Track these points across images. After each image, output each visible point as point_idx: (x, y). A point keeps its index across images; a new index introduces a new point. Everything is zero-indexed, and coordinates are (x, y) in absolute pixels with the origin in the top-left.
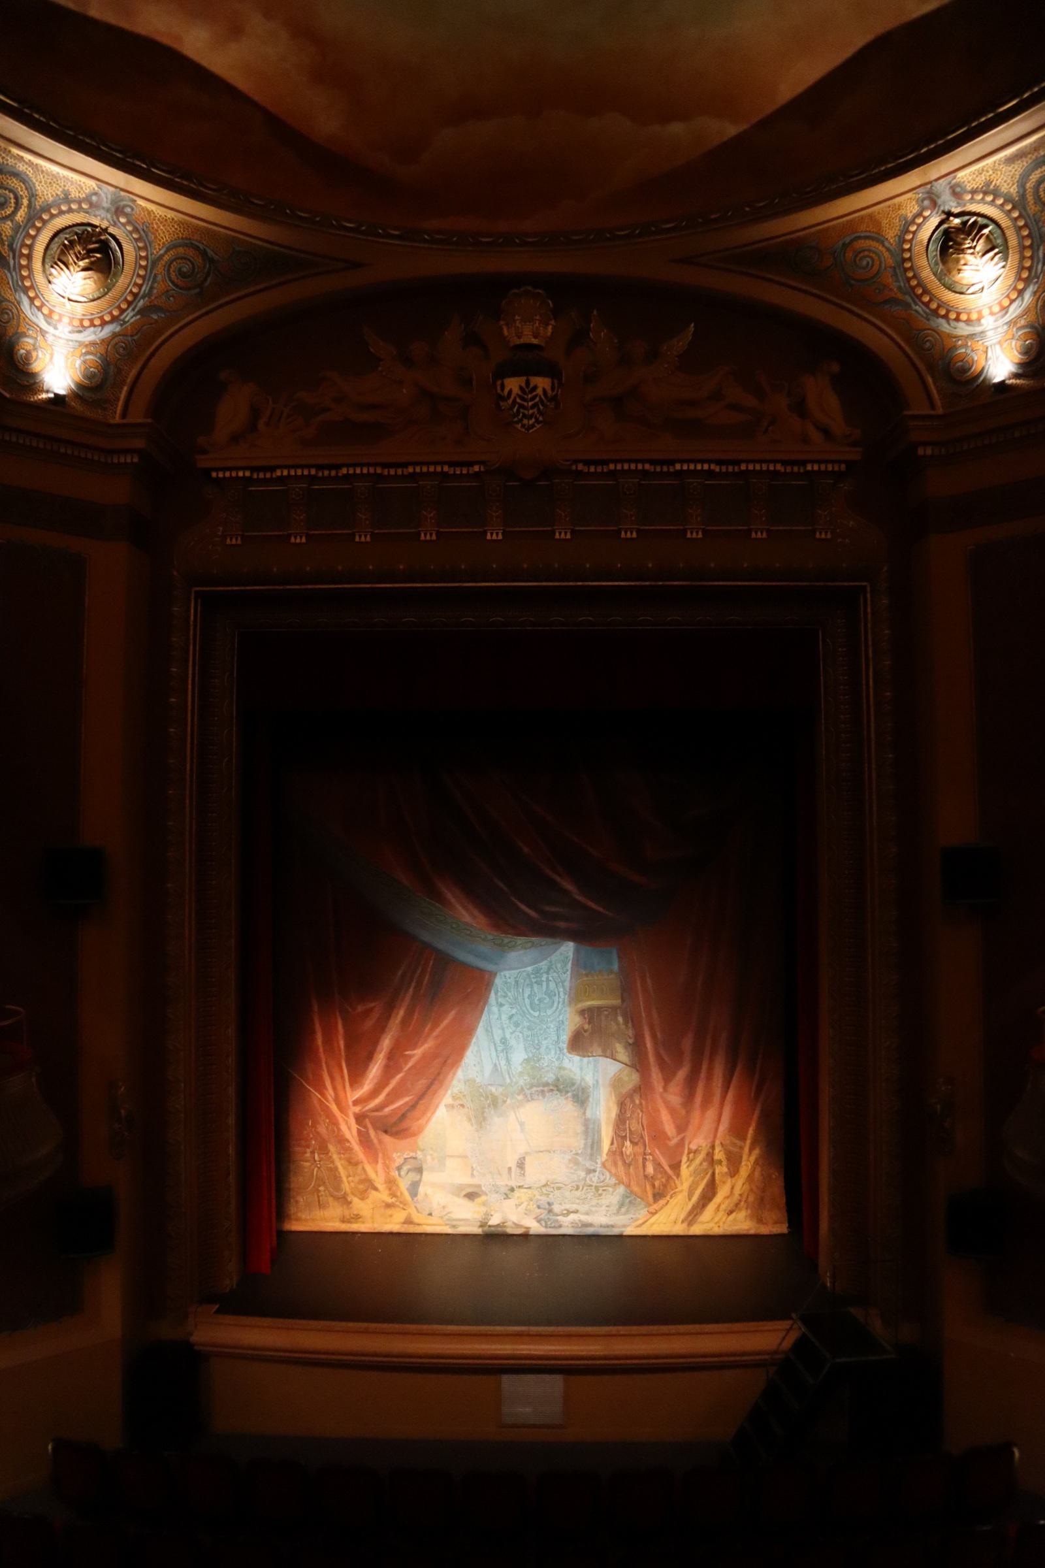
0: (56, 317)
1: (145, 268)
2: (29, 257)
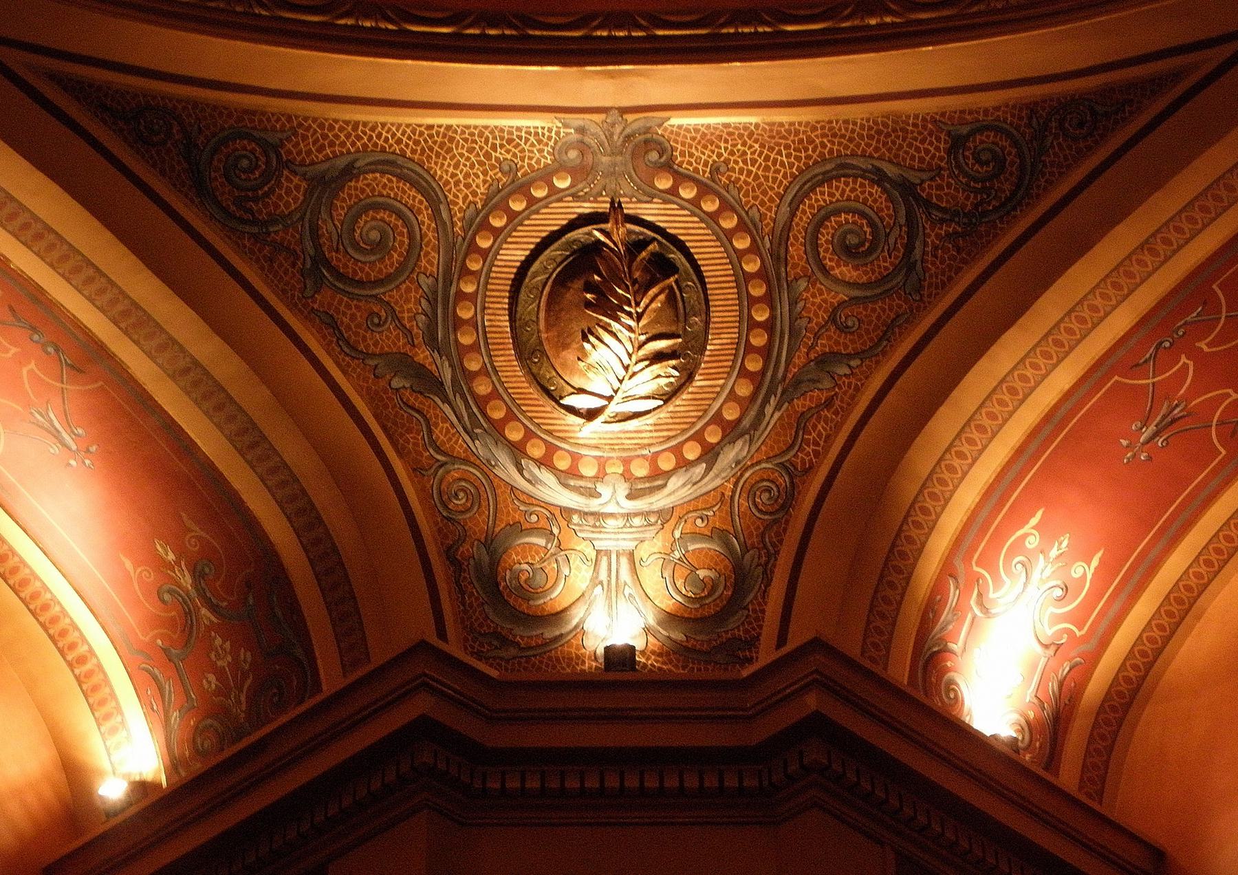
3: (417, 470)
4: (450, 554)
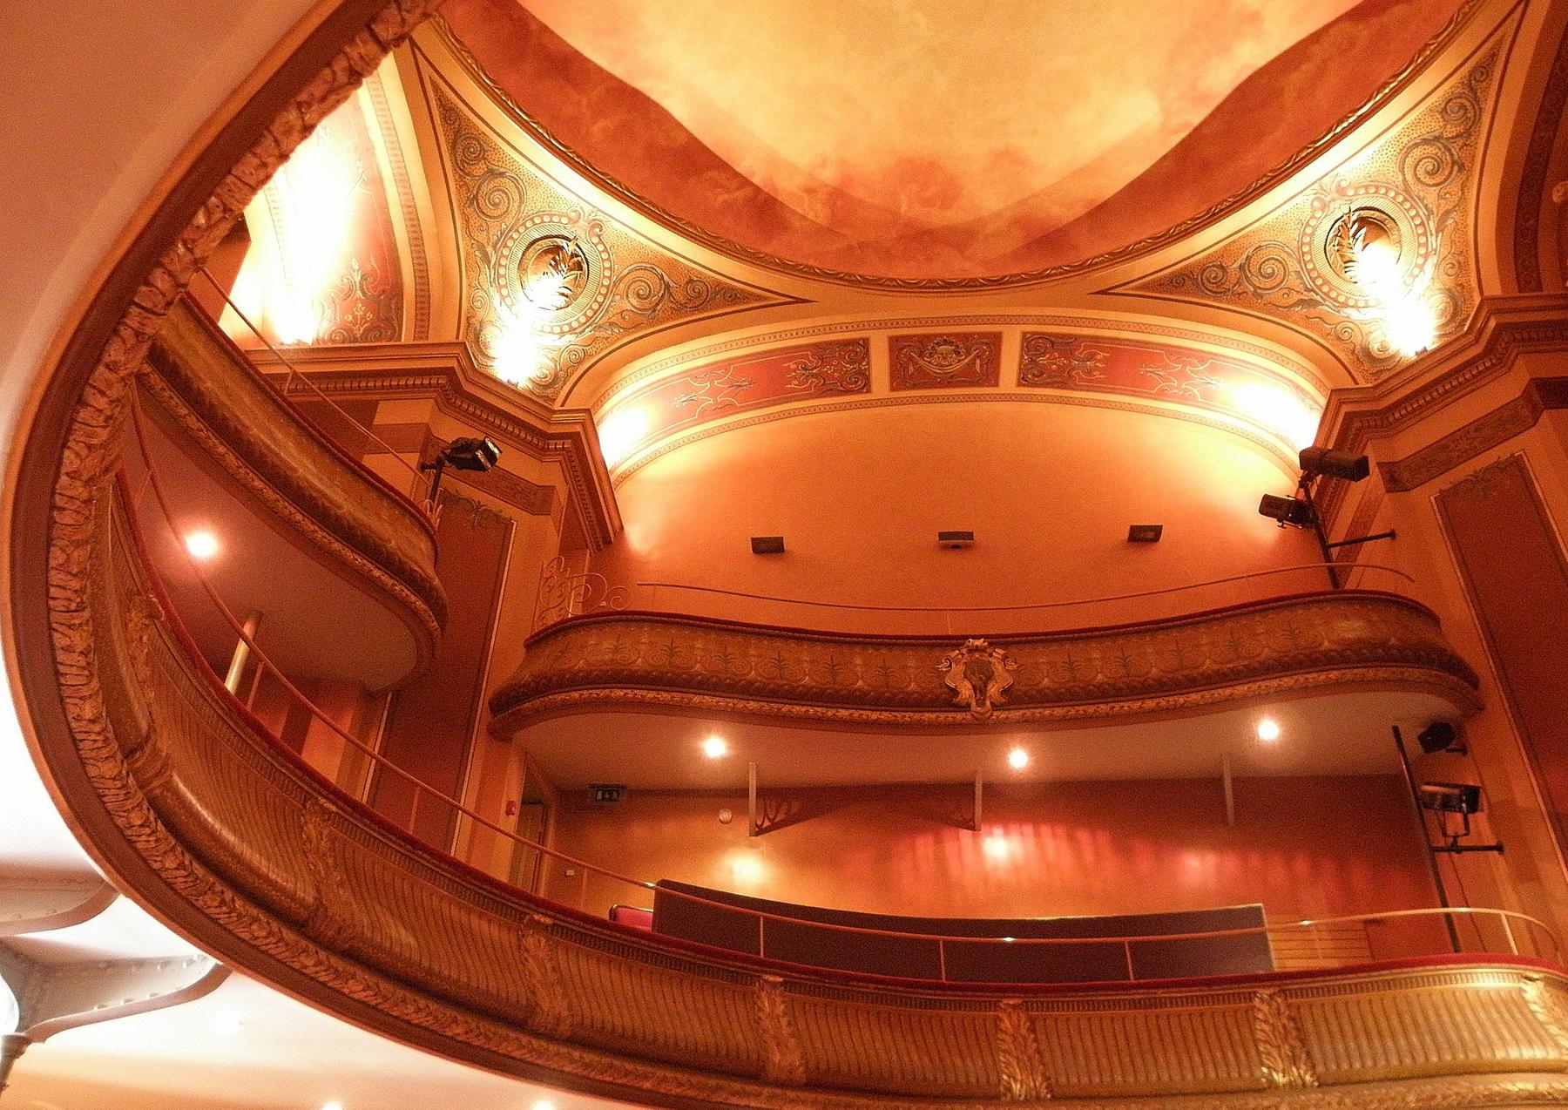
1: (1405, 200)
2: (1326, 282)
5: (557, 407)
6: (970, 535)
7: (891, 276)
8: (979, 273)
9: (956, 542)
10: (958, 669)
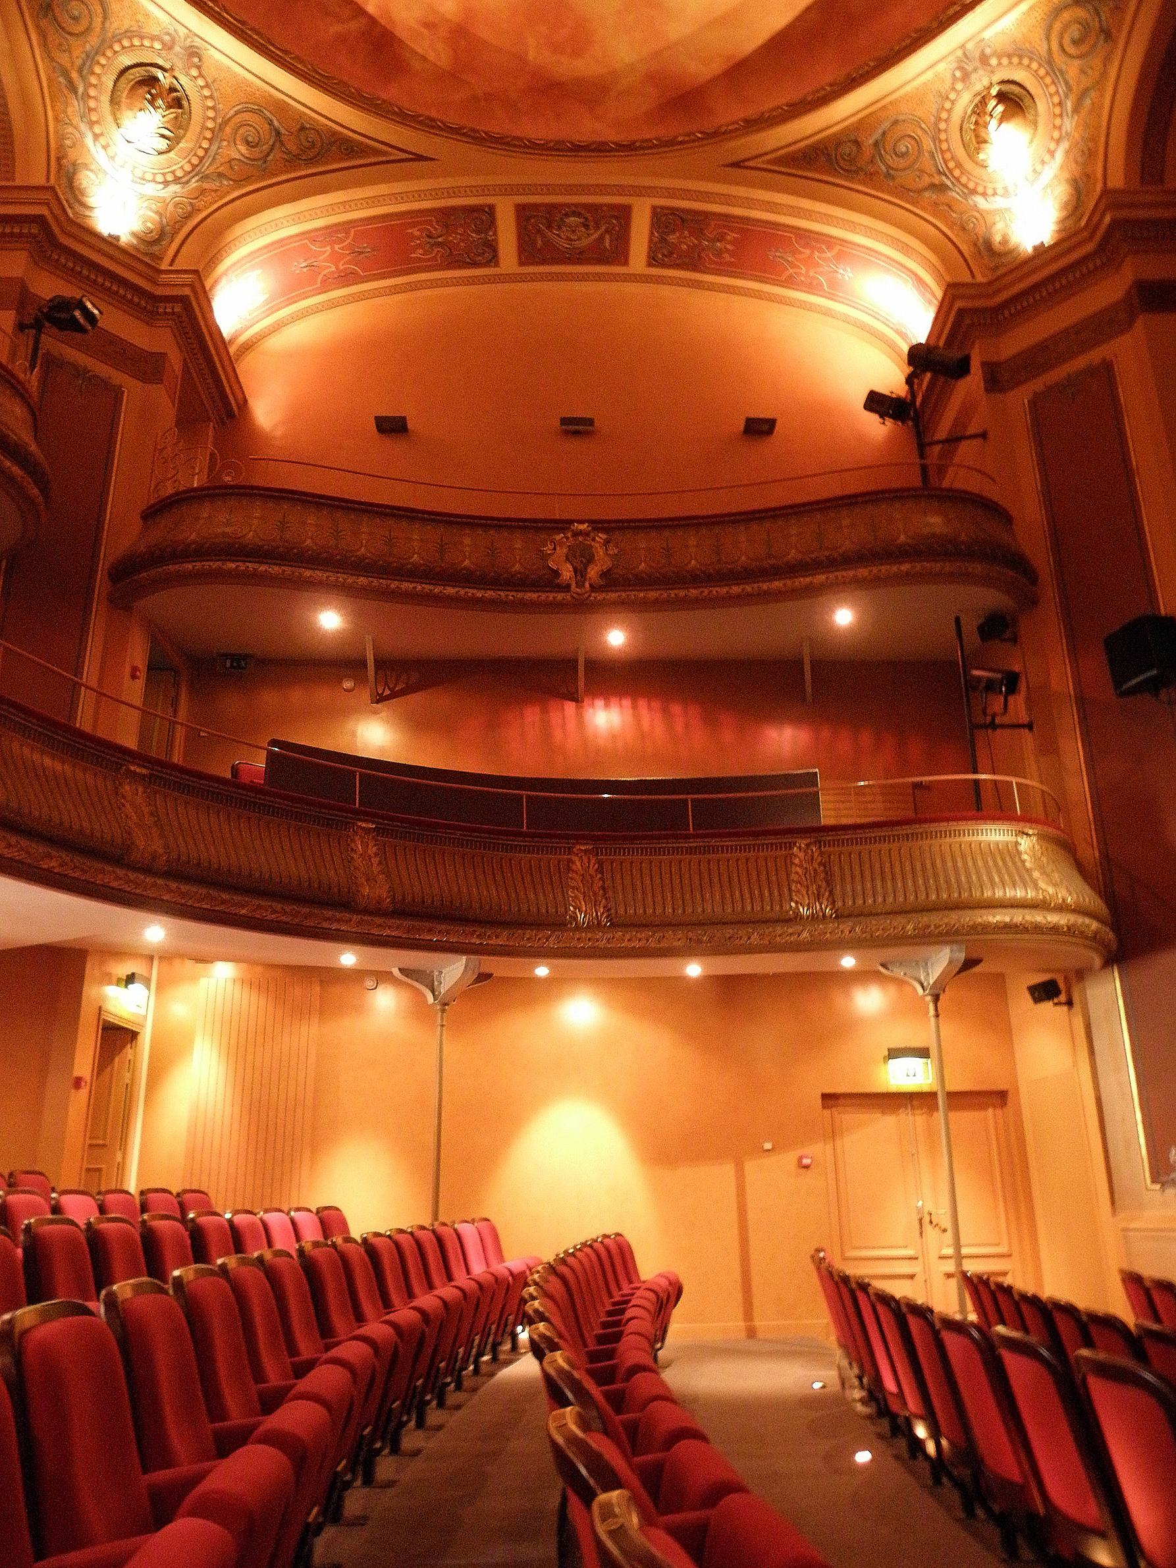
0: (1011, 190)
2: (959, 165)
3: (56, 119)
4: (58, 159)
5: (164, 266)
6: (590, 422)
7: (518, 133)
8: (611, 135)
9: (577, 428)
10: (562, 551)
